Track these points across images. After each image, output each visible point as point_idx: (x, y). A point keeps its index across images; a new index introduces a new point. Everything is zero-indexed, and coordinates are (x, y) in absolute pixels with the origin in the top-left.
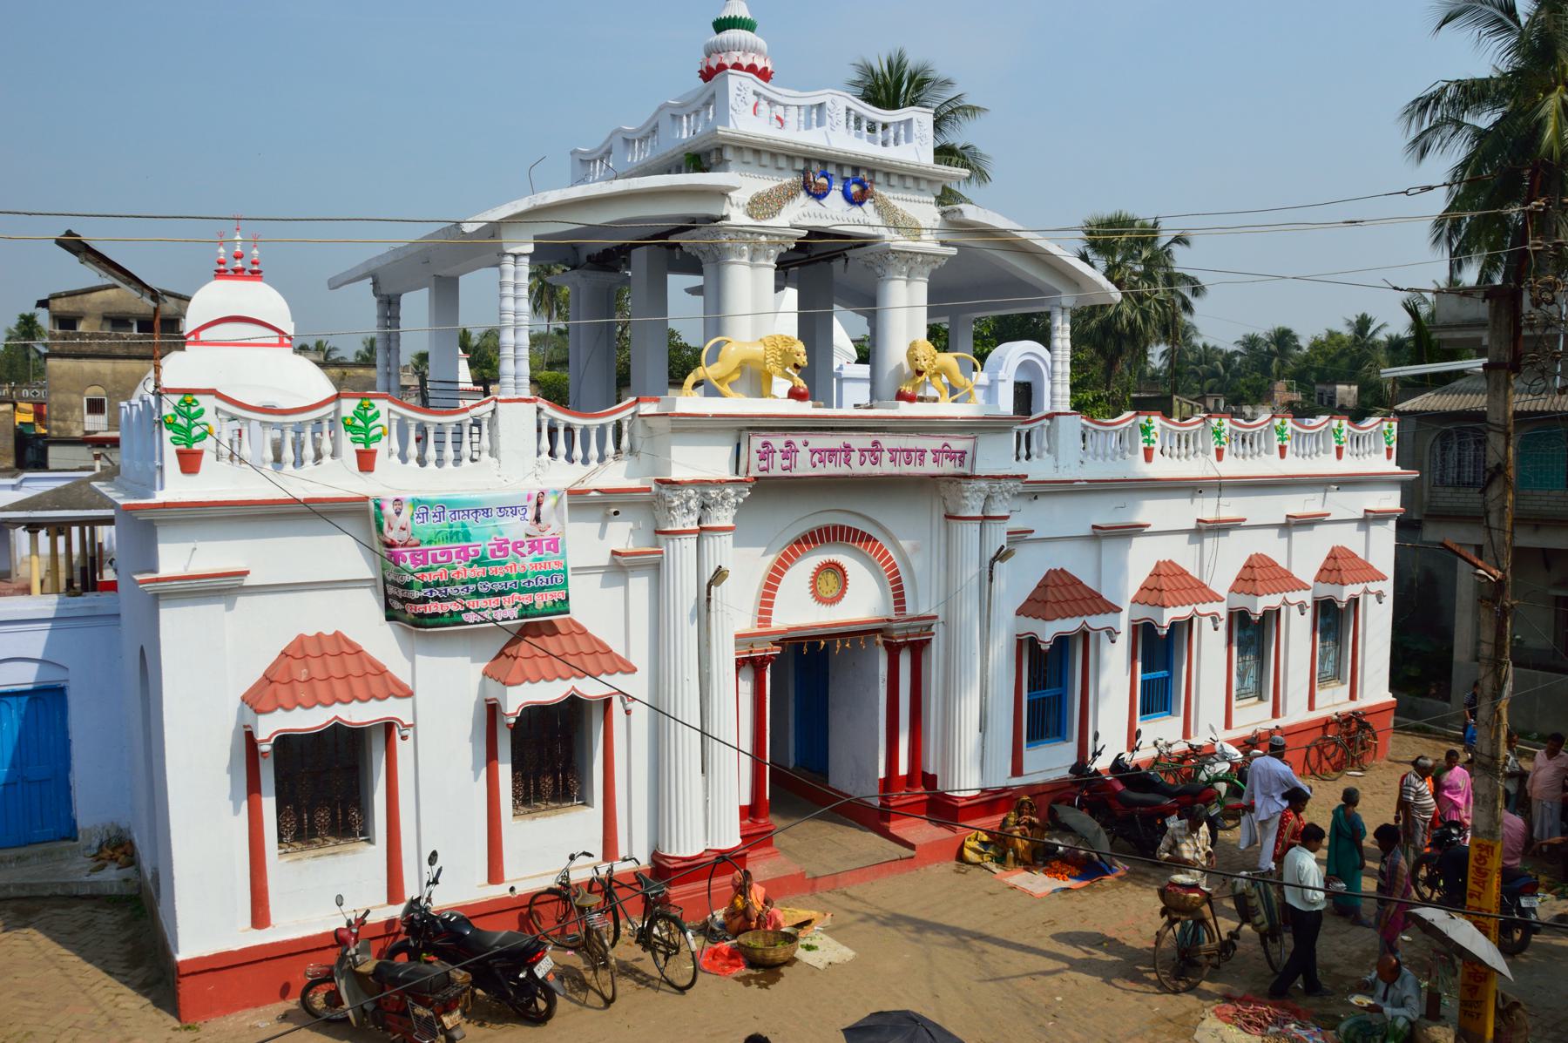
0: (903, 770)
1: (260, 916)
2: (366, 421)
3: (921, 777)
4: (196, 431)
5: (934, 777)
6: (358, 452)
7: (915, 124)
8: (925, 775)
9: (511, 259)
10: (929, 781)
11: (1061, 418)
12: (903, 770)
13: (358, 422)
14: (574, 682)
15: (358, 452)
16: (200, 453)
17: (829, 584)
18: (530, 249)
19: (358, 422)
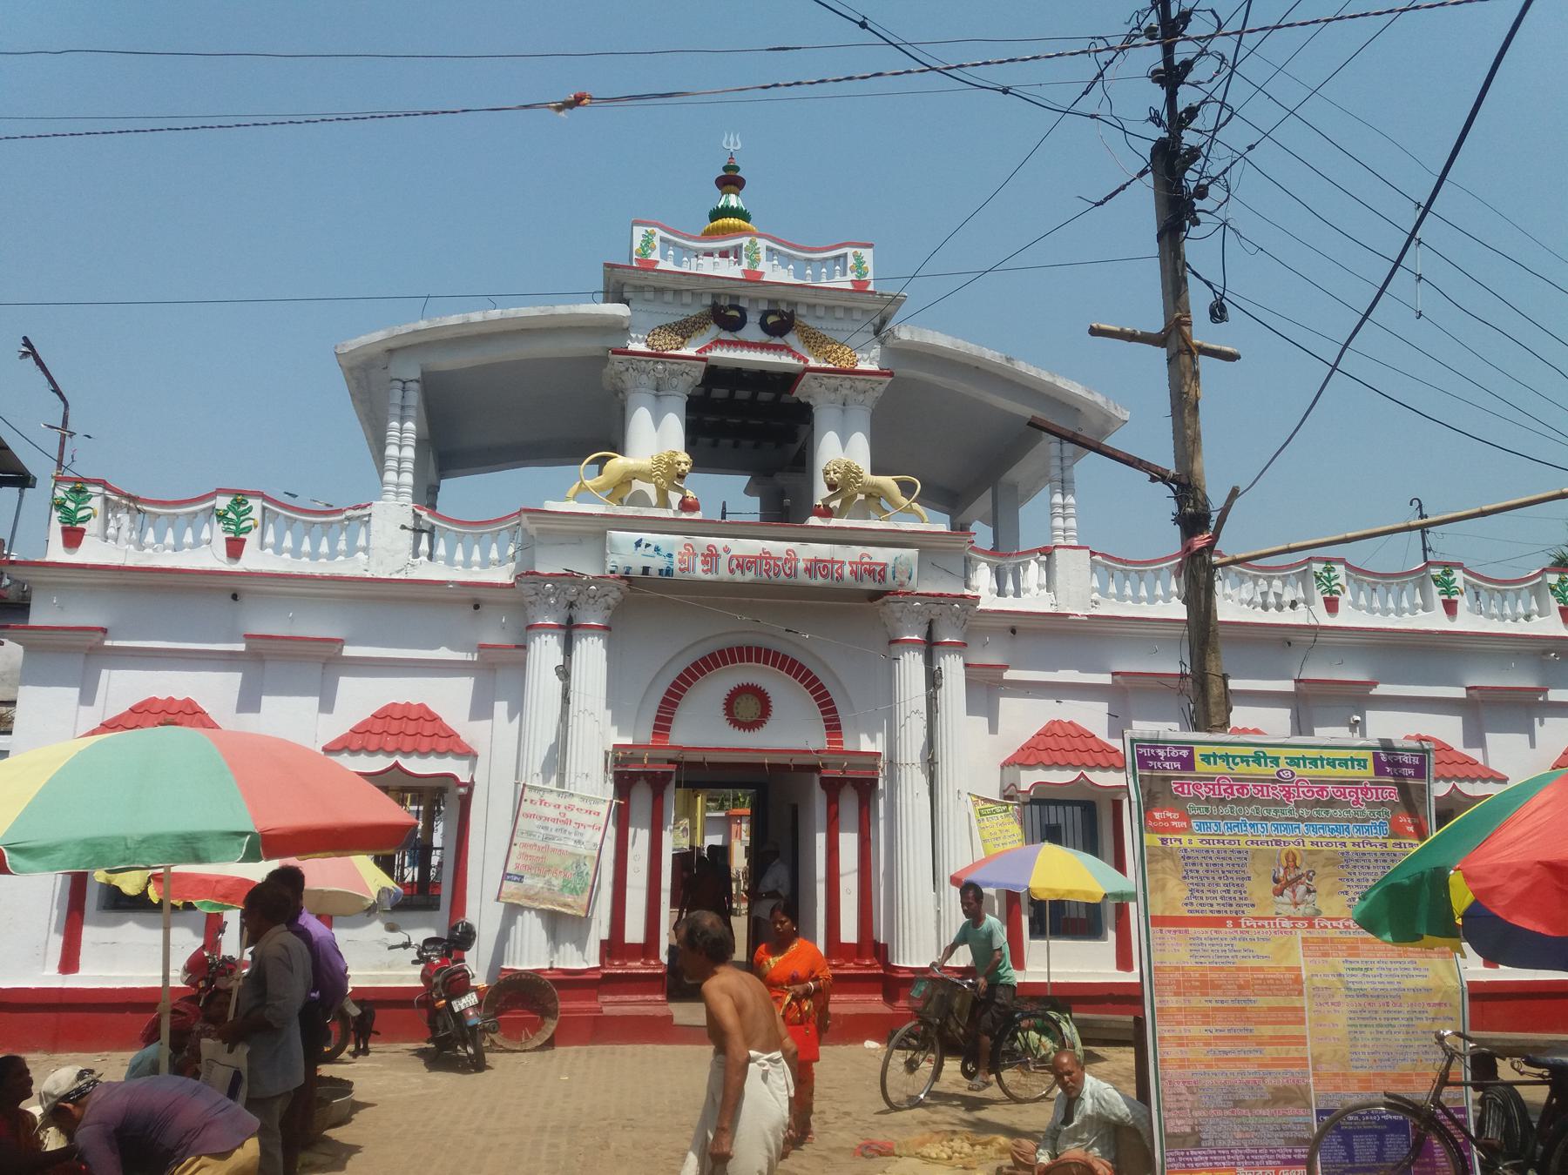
0: (849, 933)
1: (69, 962)
2: (239, 515)
3: (873, 948)
4: (80, 514)
5: (885, 946)
6: (228, 540)
7: (851, 261)
8: (877, 945)
9: (400, 384)
10: (881, 952)
11: (1057, 551)
12: (849, 933)
13: (230, 515)
14: (398, 758)
15: (228, 540)
16: (83, 531)
17: (748, 708)
18: (417, 375)
19: (230, 515)
